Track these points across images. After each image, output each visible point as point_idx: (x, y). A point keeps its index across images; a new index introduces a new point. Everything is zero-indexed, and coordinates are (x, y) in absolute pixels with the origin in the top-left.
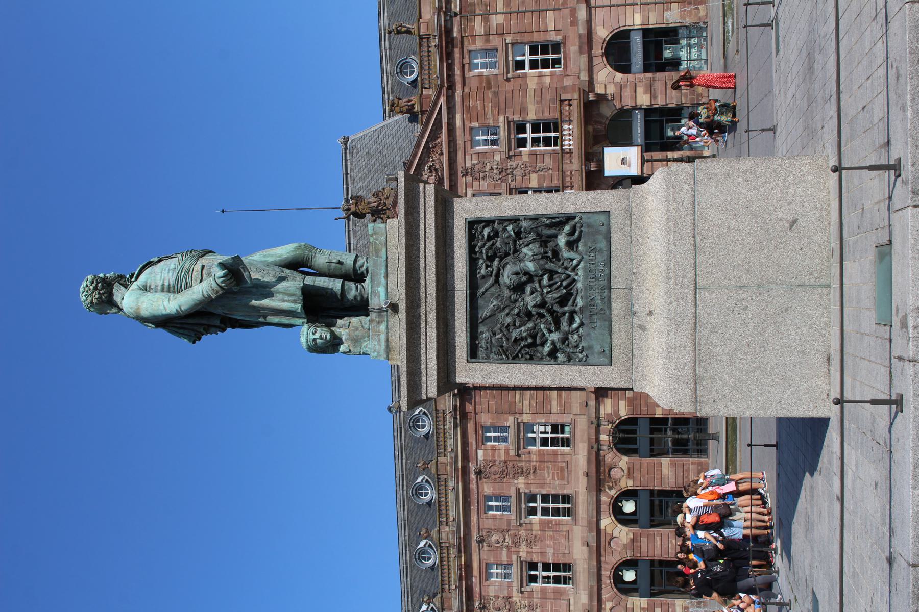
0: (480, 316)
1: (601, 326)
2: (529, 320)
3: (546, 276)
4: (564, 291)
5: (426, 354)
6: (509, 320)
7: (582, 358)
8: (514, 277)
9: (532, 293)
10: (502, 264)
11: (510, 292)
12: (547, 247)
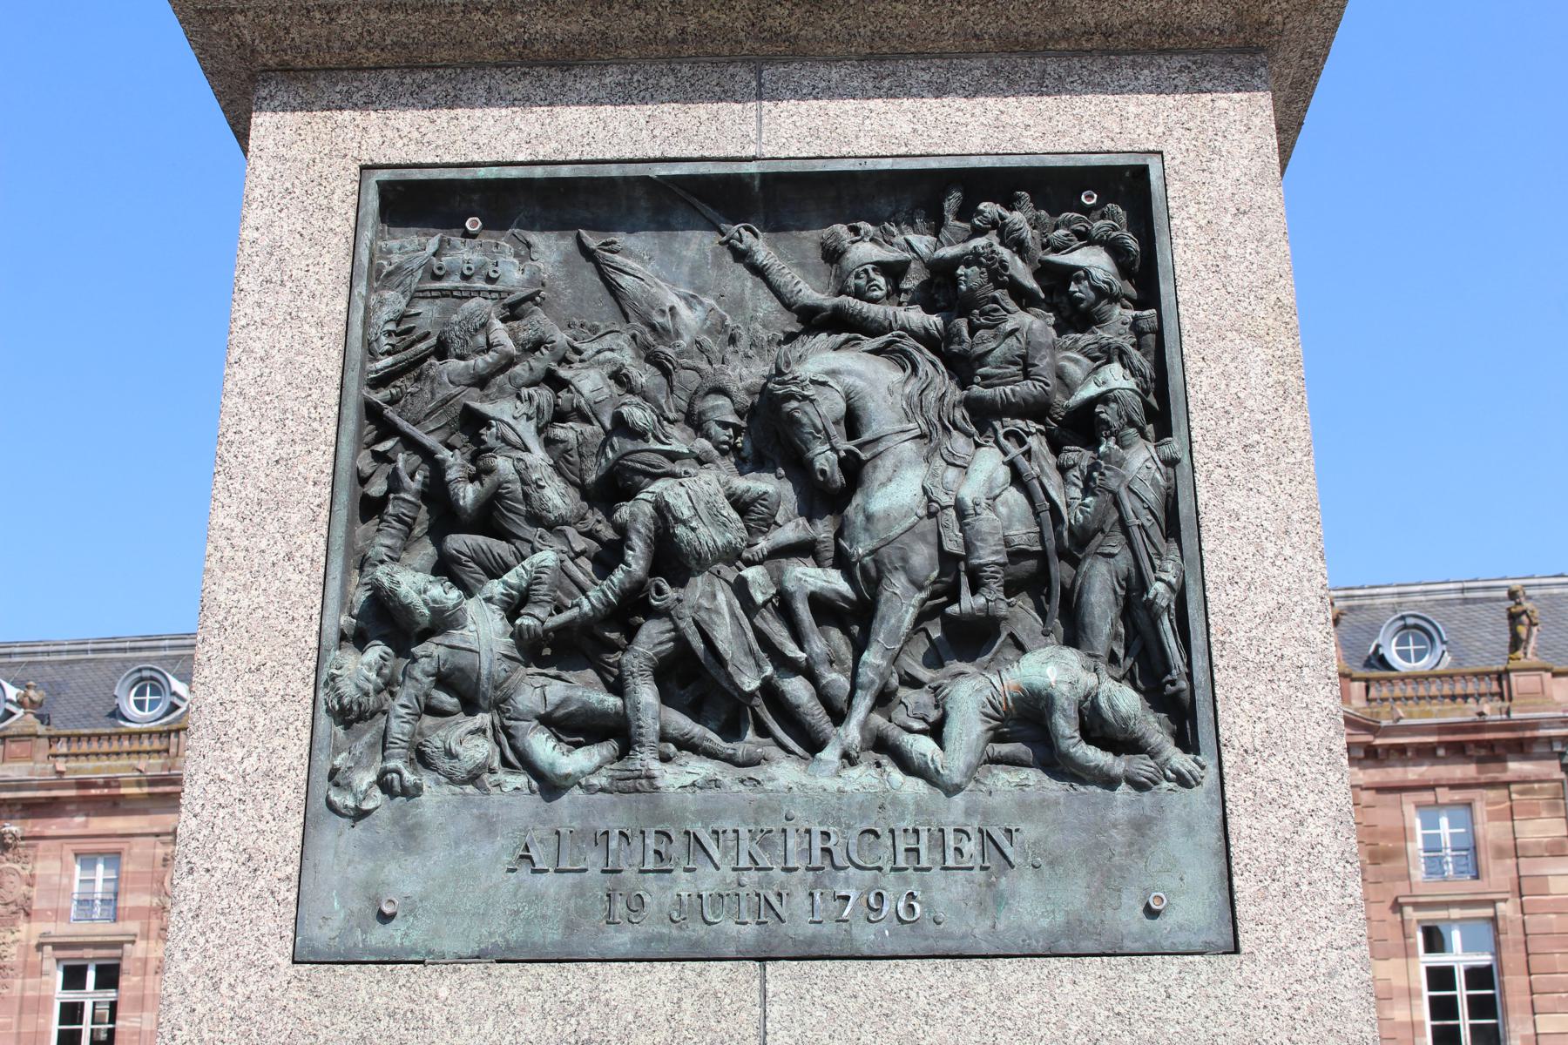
0: (620, 238)
1: (537, 898)
2: (586, 493)
3: (844, 587)
4: (750, 683)
6: (589, 383)
7: (347, 787)
8: (831, 405)
9: (742, 505)
10: (909, 344)
11: (750, 392)
12: (1011, 589)
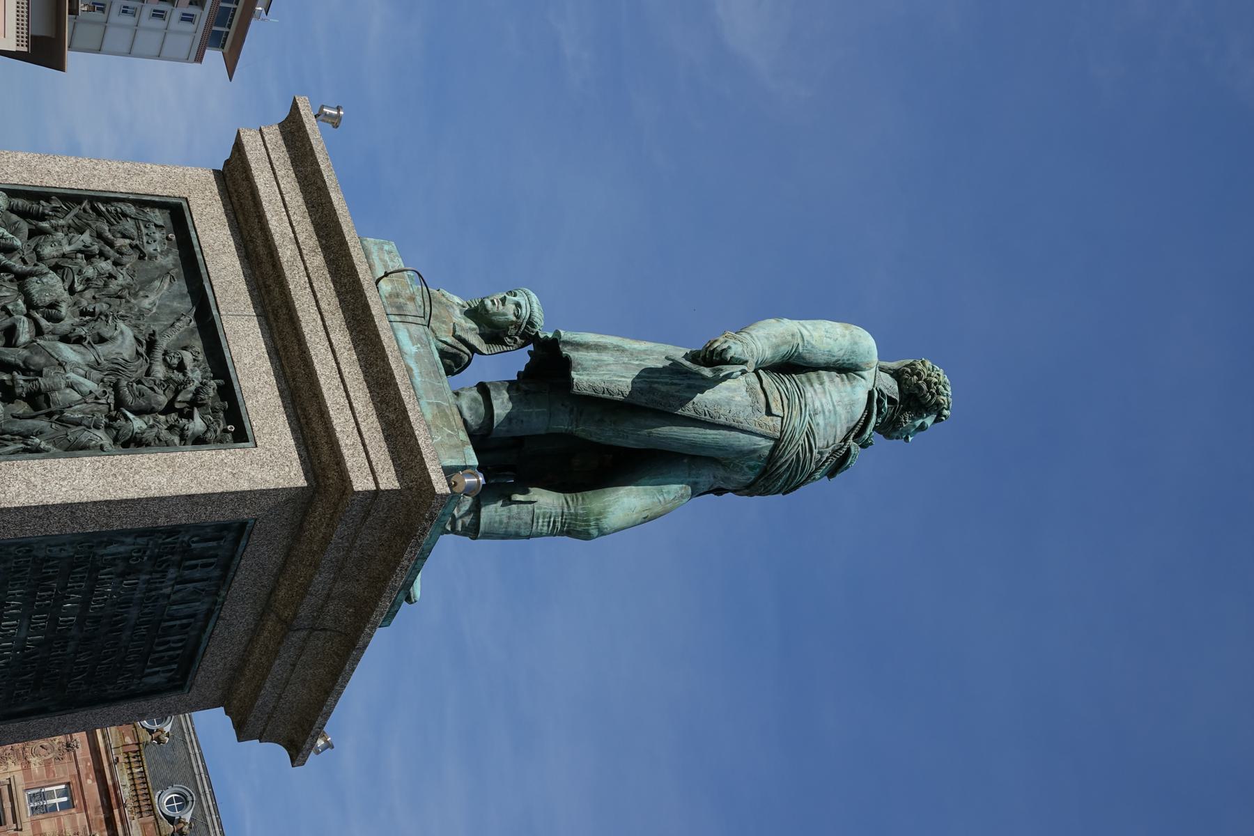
5: (281, 193)
8: (106, 332)
9: (54, 305)
